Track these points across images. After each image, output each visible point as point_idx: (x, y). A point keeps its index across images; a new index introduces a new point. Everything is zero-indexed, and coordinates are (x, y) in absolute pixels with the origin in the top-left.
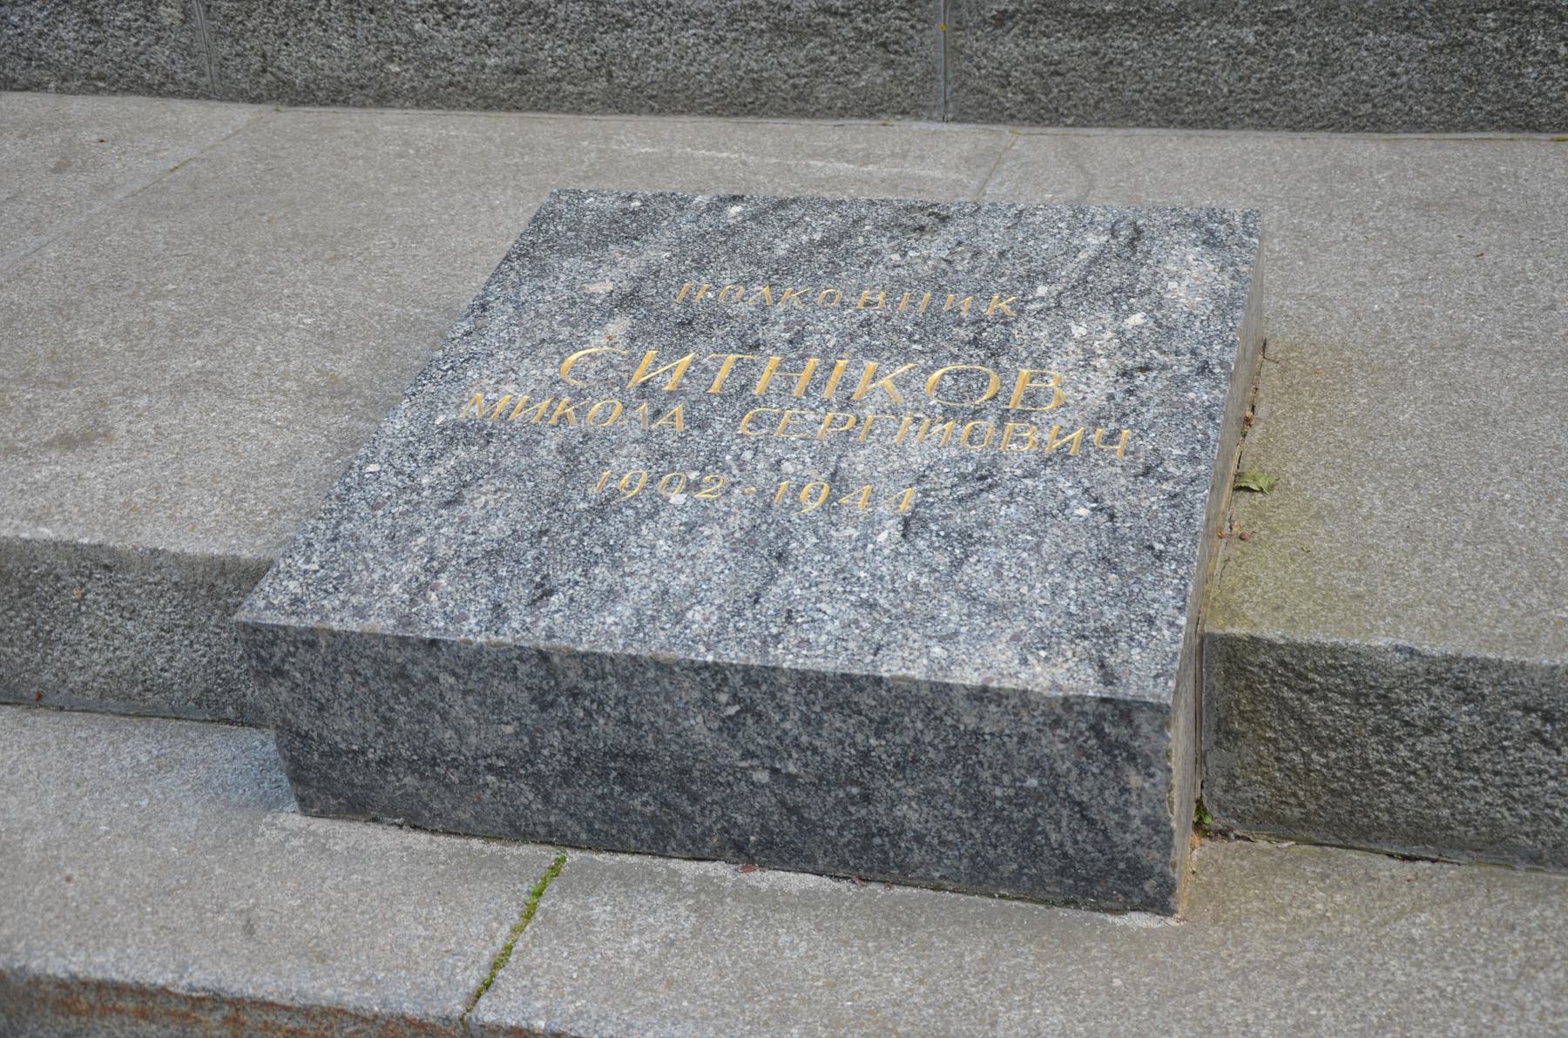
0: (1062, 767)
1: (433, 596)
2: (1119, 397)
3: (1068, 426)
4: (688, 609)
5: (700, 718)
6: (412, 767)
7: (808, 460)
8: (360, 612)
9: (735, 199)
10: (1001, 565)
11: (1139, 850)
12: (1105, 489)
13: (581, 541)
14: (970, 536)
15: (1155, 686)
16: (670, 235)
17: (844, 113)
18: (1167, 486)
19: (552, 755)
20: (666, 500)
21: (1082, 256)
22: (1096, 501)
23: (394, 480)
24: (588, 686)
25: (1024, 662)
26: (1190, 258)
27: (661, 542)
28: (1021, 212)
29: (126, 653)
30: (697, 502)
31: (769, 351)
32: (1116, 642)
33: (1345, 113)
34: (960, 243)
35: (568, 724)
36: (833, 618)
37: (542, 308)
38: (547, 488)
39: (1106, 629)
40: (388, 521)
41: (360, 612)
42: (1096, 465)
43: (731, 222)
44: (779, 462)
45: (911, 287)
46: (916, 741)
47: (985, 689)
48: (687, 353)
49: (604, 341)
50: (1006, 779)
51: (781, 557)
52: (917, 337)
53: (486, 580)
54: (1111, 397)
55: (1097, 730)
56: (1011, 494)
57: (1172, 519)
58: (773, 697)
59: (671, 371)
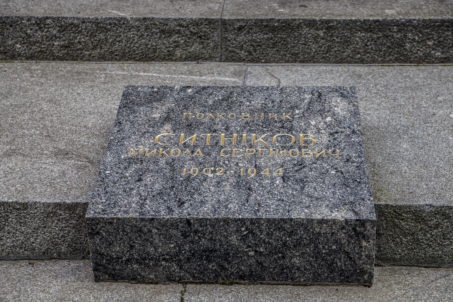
0: (343, 241)
2: (332, 141)
3: (320, 149)
5: (235, 237)
6: (137, 262)
8: (126, 212)
9: (189, 87)
10: (315, 188)
11: (364, 266)
12: (337, 166)
13: (186, 189)
14: (303, 180)
15: (370, 215)
16: (171, 99)
17: (186, 59)
18: (355, 164)
19: (185, 253)
20: (207, 176)
21: (306, 101)
22: (336, 169)
24: (201, 229)
25: (332, 212)
26: (339, 101)
27: (211, 187)
28: (282, 89)
29: (20, 238)
30: (217, 176)
31: (220, 132)
32: (355, 205)
33: (352, 58)
34: (266, 99)
35: (192, 242)
36: (272, 204)
37: (140, 123)
38: (168, 175)
39: (351, 202)
40: (122, 187)
41: (126, 212)
43: (190, 94)
44: (237, 163)
45: (256, 112)
46: (301, 237)
47: (323, 220)
48: (194, 134)
50: (326, 247)
51: (249, 189)
52: (264, 126)
53: (162, 201)
54: (329, 141)
55: (354, 229)
56: (311, 169)
57: (359, 173)
58: (259, 227)
59: (191, 139)
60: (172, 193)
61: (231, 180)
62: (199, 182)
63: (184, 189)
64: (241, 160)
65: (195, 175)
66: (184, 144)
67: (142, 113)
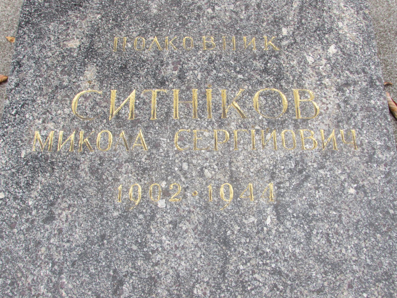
2: (342, 105)
4: (194, 286)
7: (215, 167)
10: (328, 234)
12: (356, 173)
13: (124, 241)
18: (382, 168)
20: (156, 205)
22: (356, 183)
23: (15, 205)
27: (164, 238)
30: (171, 205)
36: (264, 284)
39: (386, 273)
40: (22, 236)
42: (347, 156)
45: (224, 32)
48: (131, 91)
49: (87, 84)
51: (226, 242)
52: (238, 69)
54: (339, 106)
56: (317, 181)
57: (391, 192)
59: (127, 105)
60: (102, 254)
61: (195, 218)
62: (143, 221)
63: (121, 243)
64: (207, 159)
65: (137, 202)
66: (118, 117)
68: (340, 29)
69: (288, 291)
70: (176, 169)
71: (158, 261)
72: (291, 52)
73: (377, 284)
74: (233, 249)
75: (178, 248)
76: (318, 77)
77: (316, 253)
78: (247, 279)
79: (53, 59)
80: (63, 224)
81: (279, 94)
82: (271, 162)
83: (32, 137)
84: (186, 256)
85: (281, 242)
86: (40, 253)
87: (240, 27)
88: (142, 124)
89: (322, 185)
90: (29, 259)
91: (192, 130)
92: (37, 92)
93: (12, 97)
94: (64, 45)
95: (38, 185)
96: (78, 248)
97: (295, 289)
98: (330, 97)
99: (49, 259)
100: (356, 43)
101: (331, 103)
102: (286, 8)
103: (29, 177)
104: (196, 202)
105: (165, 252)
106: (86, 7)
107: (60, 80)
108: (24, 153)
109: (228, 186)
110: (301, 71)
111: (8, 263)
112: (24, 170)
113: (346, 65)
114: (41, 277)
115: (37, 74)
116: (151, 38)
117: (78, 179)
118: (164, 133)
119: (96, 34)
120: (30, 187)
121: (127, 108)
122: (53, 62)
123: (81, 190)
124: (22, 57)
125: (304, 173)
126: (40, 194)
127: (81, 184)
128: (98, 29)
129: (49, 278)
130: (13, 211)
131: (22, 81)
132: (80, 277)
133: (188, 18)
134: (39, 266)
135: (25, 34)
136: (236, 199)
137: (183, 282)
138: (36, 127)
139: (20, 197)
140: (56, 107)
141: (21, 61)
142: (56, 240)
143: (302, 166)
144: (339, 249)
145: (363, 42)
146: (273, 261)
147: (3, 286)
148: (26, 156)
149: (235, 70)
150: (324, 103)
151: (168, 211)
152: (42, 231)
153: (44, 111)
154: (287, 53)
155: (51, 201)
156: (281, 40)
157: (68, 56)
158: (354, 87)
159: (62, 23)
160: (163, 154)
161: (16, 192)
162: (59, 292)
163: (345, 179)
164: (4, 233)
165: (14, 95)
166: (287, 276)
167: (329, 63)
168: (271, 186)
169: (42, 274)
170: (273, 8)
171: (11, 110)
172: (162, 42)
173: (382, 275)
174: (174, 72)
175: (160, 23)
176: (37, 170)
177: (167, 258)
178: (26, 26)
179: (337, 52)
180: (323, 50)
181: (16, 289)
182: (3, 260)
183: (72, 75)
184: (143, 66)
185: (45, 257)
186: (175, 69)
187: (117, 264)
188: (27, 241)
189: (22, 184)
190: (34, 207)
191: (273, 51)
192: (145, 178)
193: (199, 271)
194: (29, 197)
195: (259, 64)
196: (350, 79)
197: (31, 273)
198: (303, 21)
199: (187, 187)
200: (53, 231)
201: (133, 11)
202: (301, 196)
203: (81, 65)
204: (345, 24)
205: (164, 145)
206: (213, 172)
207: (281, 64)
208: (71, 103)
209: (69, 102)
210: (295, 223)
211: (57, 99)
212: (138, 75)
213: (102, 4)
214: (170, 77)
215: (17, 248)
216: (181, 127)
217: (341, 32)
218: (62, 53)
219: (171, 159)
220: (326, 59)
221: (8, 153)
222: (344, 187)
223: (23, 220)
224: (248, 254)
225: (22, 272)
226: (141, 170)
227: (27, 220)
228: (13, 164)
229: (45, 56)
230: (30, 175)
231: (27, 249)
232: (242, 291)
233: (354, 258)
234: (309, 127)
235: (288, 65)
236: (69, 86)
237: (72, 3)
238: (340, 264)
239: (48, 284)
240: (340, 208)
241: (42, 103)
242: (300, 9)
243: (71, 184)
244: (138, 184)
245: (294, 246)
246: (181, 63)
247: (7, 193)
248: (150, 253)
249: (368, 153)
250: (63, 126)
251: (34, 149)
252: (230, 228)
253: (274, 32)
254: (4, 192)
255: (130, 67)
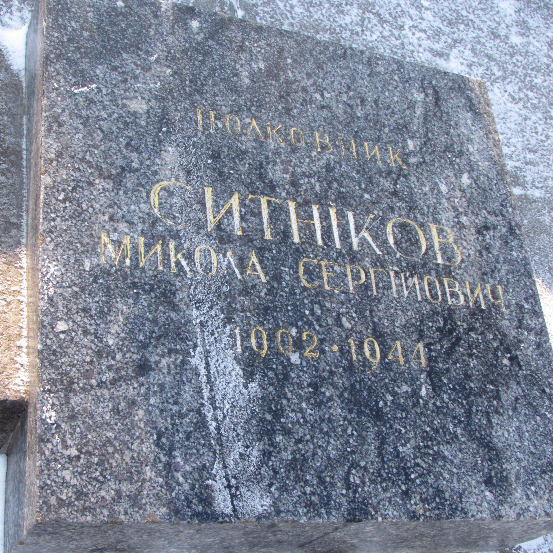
1: (179, 475)
7: (354, 315)
20: (289, 359)
26: (469, 122)
30: (308, 362)
43: (199, 38)
64: (342, 303)
65: (263, 353)
67: (104, 92)
68: (471, 154)
69: (455, 481)
70: (307, 312)
71: (302, 437)
72: (421, 174)
73: (543, 475)
74: (388, 426)
75: (324, 420)
76: (454, 212)
77: (479, 435)
78: (409, 465)
79: (110, 123)
80: (165, 377)
81: (415, 228)
82: (417, 316)
83: (96, 240)
84: (334, 431)
85: (440, 420)
86: (136, 418)
87: (358, 127)
88: (255, 242)
89: (475, 351)
90: (122, 427)
91: (319, 261)
92: (93, 170)
93: (54, 172)
94: (124, 105)
95: (118, 315)
96: (191, 414)
97: (462, 478)
98: (470, 240)
99: (153, 428)
100: (490, 175)
101: (473, 248)
102: (408, 112)
103: (102, 301)
104: (338, 360)
105: (309, 425)
106: (147, 52)
107: (125, 157)
108: (89, 264)
109: (373, 342)
110: (435, 201)
111: (90, 431)
112: (93, 290)
113: (483, 203)
114: (144, 454)
115: (89, 142)
116: (248, 120)
117: (176, 312)
118: (284, 260)
119: (170, 97)
120: (106, 317)
121: (230, 217)
122: (111, 129)
123: (183, 329)
124: (60, 111)
125: (454, 334)
126: (123, 330)
127: (183, 321)
128: (171, 90)
129: (156, 456)
130: (85, 352)
131: (67, 149)
132: (201, 455)
133: (292, 102)
134: (138, 438)
135: (58, 74)
136: (384, 360)
137: (335, 466)
138: (101, 225)
139: (92, 331)
140: (127, 199)
141: (59, 116)
142: (159, 401)
143: (450, 324)
144: (502, 431)
145: (497, 175)
146: (435, 443)
147: (88, 467)
148: (92, 269)
149: (360, 186)
150: (464, 248)
151: (305, 369)
152: (136, 385)
153: (109, 202)
154: (417, 174)
155: (141, 341)
156: (408, 155)
157: (132, 123)
158: (494, 232)
159: (115, 69)
160: (287, 290)
161: (85, 323)
162: (173, 476)
163: (498, 346)
164: (76, 385)
165: (57, 170)
166: (452, 462)
167: (464, 197)
168: (420, 346)
169: (144, 449)
170: (393, 110)
171: (56, 194)
172: (263, 128)
173: (547, 466)
174: (285, 176)
175: (256, 99)
176: (112, 292)
177: (312, 433)
178: (57, 61)
179: (471, 184)
180: (456, 178)
181: (108, 472)
182: (81, 426)
183: (144, 154)
184: (242, 159)
185: (146, 424)
186: (285, 171)
187: (249, 439)
188: (114, 398)
189: (93, 312)
190: (118, 349)
191: (401, 169)
192: (269, 320)
193: (353, 452)
194: (108, 332)
195: (387, 184)
196: (488, 221)
197: (128, 448)
198: (430, 135)
199: (324, 339)
200: (152, 386)
201: (217, 75)
202: (455, 363)
203: (154, 141)
204: (476, 149)
205: (287, 278)
206: (353, 322)
207: (412, 188)
208: (148, 197)
209: (144, 194)
210: (453, 397)
211: (126, 187)
212: (238, 171)
213: (170, 53)
214: (281, 182)
215: (101, 409)
216: (304, 255)
217: (472, 158)
218: (123, 117)
219: (298, 297)
220: (460, 190)
221: (63, 261)
222: (498, 356)
223: (103, 367)
224: (406, 432)
225: (114, 446)
226: (263, 309)
227: (109, 368)
228: (73, 278)
229: (97, 117)
230: (103, 299)
231: (116, 411)
232: (405, 480)
233: (518, 444)
234: (453, 277)
235: (420, 191)
236: (142, 171)
237: (126, 41)
238: (505, 450)
239: (156, 464)
240: (496, 381)
241: (104, 189)
242: (424, 118)
243: (167, 319)
244: (260, 329)
245: (455, 426)
246: (292, 164)
247: (71, 324)
248: (290, 425)
249: (517, 317)
250: (142, 230)
251: (103, 260)
252: (381, 397)
253: (398, 142)
254: (65, 321)
255: (224, 158)
